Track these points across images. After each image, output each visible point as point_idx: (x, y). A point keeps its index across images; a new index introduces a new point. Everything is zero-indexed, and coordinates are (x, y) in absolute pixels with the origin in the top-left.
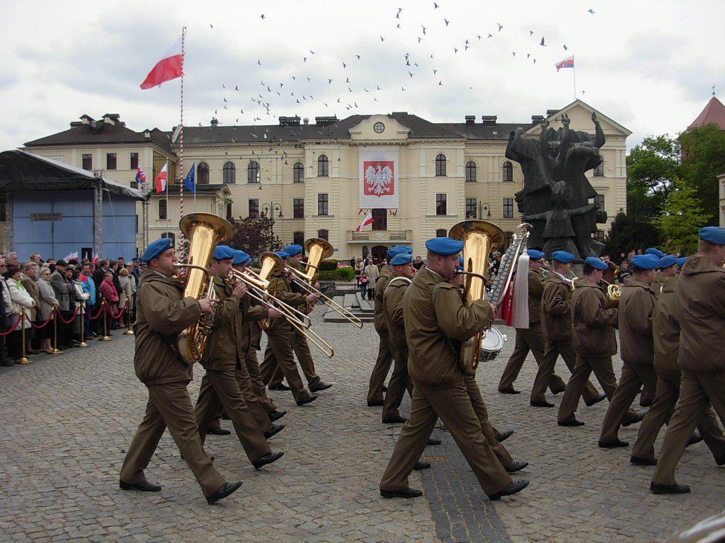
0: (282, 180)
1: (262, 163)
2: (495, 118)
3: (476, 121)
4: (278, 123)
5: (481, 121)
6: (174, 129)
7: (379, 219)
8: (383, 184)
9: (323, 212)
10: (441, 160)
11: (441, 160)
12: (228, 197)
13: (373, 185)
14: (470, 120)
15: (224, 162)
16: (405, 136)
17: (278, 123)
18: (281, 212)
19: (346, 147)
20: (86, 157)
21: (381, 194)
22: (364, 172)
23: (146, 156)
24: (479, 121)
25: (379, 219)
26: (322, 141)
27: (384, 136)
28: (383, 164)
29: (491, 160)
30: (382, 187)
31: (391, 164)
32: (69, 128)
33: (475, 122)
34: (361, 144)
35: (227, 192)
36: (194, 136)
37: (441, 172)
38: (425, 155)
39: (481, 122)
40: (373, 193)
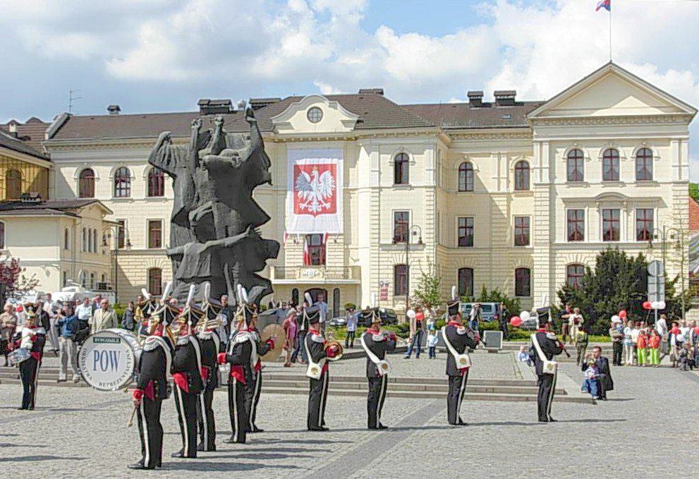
2: (514, 93)
5: (492, 100)
8: (320, 198)
11: (611, 157)
13: (306, 200)
18: (420, 238)
21: (318, 213)
22: (295, 180)
27: (321, 128)
28: (322, 169)
30: (320, 203)
31: (332, 168)
33: (483, 101)
34: (289, 140)
37: (400, 176)
39: (492, 100)
40: (306, 211)
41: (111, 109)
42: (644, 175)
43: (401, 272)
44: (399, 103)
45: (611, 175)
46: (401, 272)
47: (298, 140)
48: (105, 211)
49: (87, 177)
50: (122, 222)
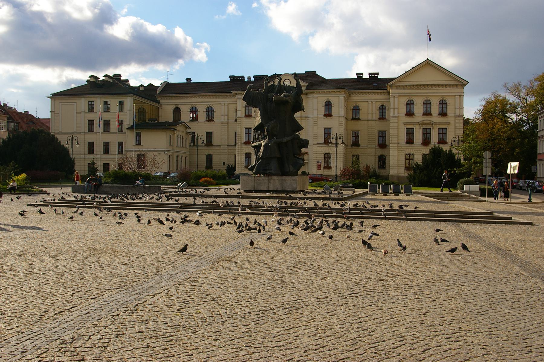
1: (215, 108)
2: (378, 74)
3: (364, 77)
4: (229, 80)
5: (368, 77)
10: (328, 105)
14: (360, 75)
15: (206, 106)
17: (229, 80)
20: (90, 103)
24: (366, 76)
29: (370, 104)
39: (368, 77)
41: (187, 79)
43: (328, 157)
44: (326, 78)
48: (187, 127)
49: (177, 111)
50: (194, 133)
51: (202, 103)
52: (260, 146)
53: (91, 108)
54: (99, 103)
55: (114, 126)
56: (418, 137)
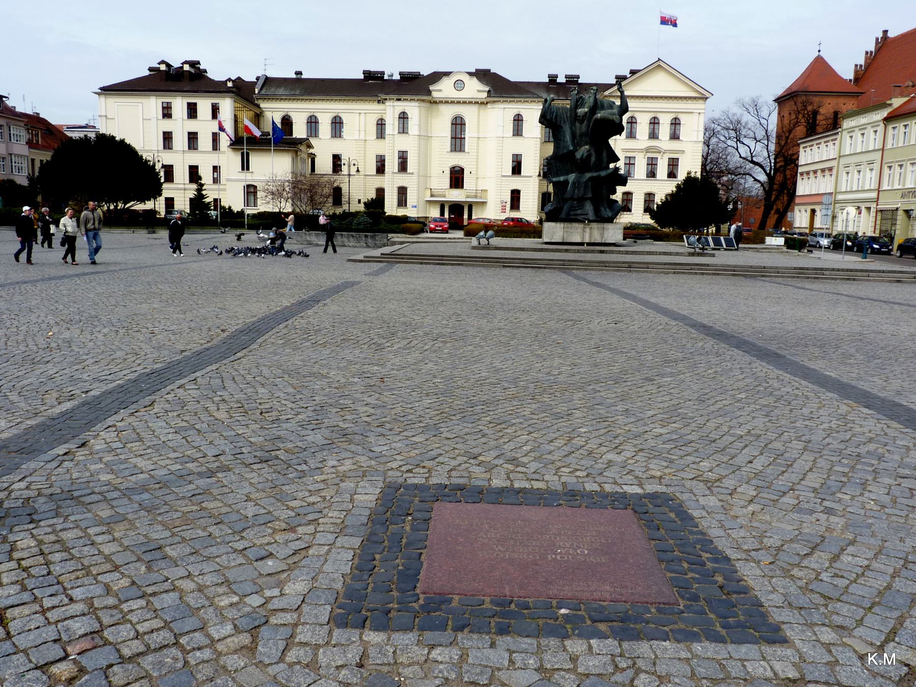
0: (365, 136)
2: (578, 77)
3: (559, 80)
4: (362, 77)
6: (258, 78)
7: (457, 178)
9: (403, 167)
10: (518, 120)
12: (311, 151)
14: (553, 79)
15: (308, 115)
16: (485, 95)
17: (362, 77)
19: (428, 105)
20: (165, 105)
23: (227, 105)
24: (561, 79)
25: (457, 178)
26: (403, 97)
32: (147, 73)
34: (441, 102)
35: (310, 146)
36: (273, 86)
37: (518, 130)
38: (501, 114)
39: (564, 80)
41: (299, 73)
42: (675, 136)
43: (515, 196)
44: (512, 79)
45: (653, 135)
46: (515, 196)
47: (447, 102)
51: (325, 110)
52: (566, 182)
53: (167, 113)
54: (179, 104)
55: (205, 142)
56: (662, 169)
